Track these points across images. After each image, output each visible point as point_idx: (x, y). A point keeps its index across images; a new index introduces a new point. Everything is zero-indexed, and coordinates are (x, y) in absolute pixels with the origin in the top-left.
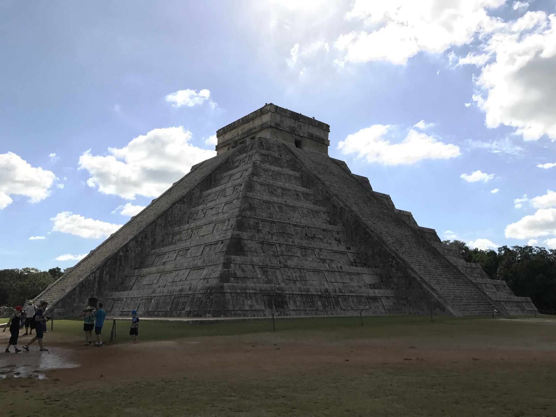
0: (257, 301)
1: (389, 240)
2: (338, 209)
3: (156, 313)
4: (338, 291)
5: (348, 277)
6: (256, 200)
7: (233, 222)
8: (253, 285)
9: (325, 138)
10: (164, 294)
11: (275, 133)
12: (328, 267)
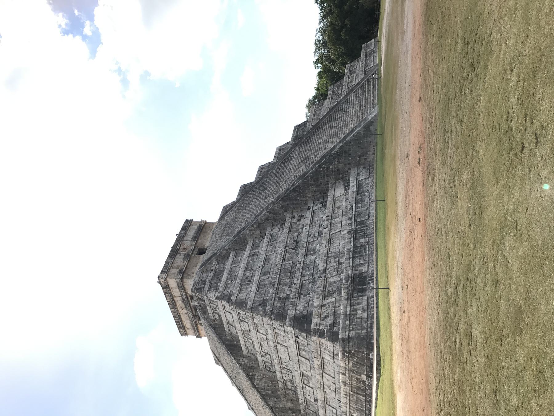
0: (358, 304)
1: (303, 169)
3: (367, 412)
4: (350, 222)
5: (336, 211)
6: (256, 299)
7: (276, 324)
8: (342, 307)
9: (198, 225)
10: (348, 402)
11: (189, 275)
12: (327, 229)
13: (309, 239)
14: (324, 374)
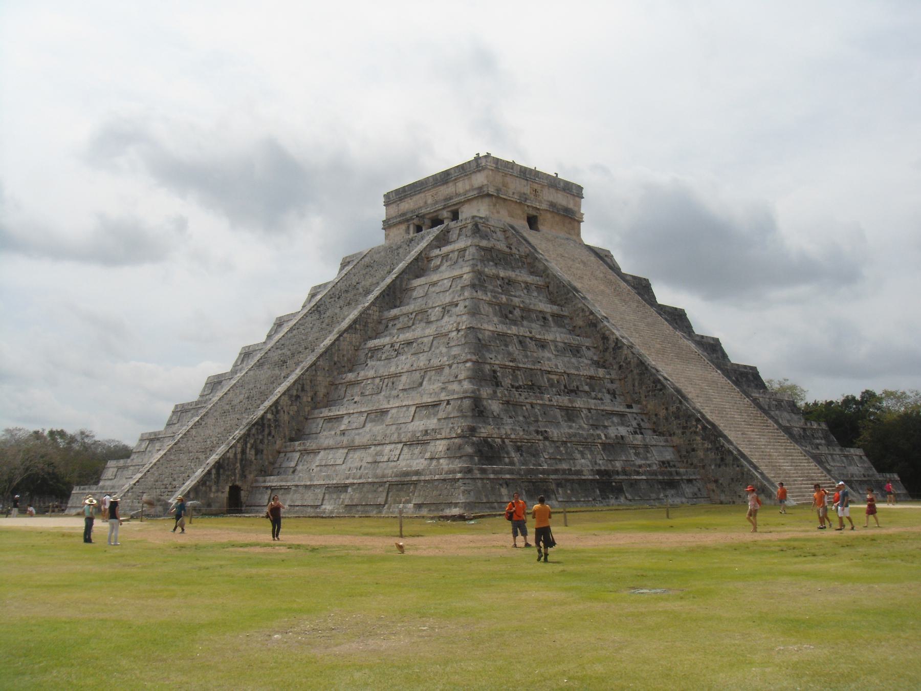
2: (611, 342)
9: (576, 209)
11: (495, 205)
14: (400, 446)
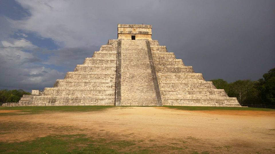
0: (44, 101)
5: (98, 92)
9: (149, 31)
11: (121, 36)
12: (89, 89)
13: (93, 83)
